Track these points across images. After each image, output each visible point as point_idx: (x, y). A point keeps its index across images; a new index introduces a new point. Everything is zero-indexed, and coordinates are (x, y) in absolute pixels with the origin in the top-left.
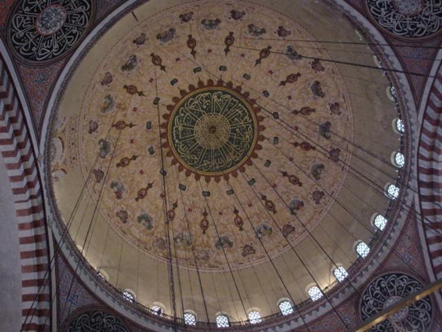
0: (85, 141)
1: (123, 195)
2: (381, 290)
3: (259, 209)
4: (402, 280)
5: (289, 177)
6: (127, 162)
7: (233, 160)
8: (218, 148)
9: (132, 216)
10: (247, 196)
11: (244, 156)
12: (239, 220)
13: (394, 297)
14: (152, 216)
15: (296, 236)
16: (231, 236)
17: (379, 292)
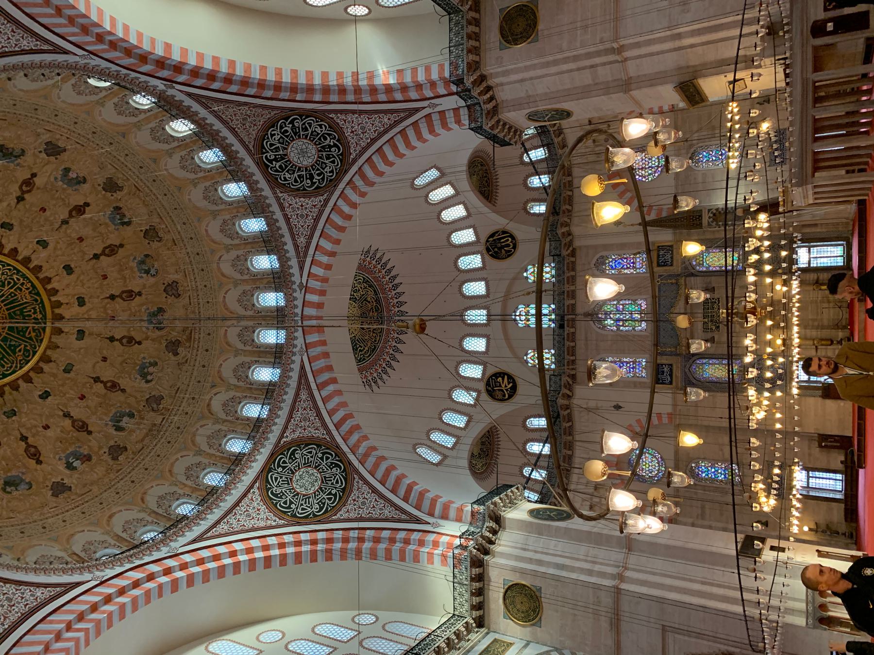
0: (12, 515)
1: (86, 453)
2: (277, 161)
3: (114, 266)
4: (272, 135)
5: (71, 216)
6: (33, 450)
7: (30, 293)
8: (6, 313)
9: (116, 439)
10: (91, 279)
11: (24, 277)
12: (124, 295)
13: (289, 150)
14: (114, 411)
15: (164, 226)
16: (148, 309)
17: (278, 164)
